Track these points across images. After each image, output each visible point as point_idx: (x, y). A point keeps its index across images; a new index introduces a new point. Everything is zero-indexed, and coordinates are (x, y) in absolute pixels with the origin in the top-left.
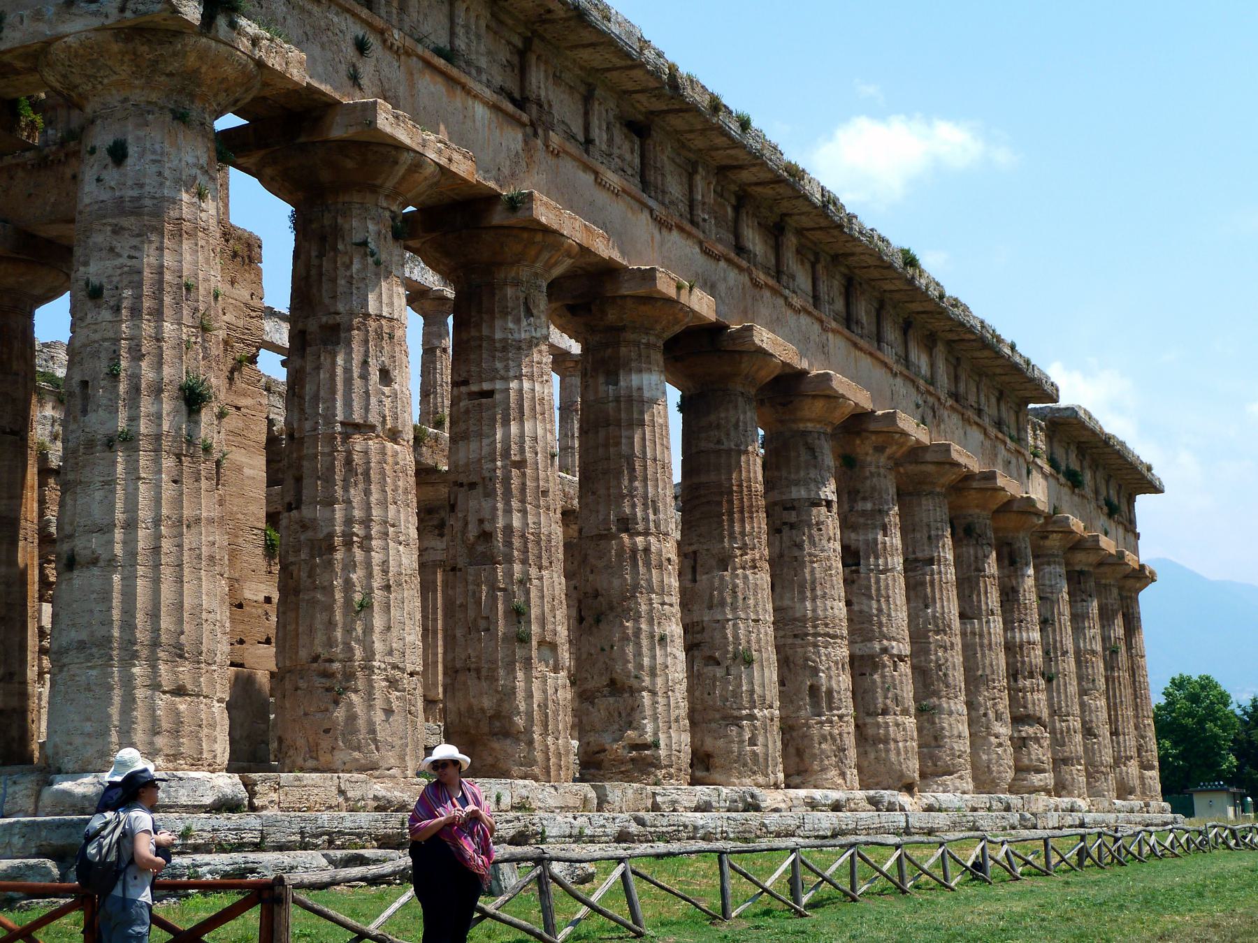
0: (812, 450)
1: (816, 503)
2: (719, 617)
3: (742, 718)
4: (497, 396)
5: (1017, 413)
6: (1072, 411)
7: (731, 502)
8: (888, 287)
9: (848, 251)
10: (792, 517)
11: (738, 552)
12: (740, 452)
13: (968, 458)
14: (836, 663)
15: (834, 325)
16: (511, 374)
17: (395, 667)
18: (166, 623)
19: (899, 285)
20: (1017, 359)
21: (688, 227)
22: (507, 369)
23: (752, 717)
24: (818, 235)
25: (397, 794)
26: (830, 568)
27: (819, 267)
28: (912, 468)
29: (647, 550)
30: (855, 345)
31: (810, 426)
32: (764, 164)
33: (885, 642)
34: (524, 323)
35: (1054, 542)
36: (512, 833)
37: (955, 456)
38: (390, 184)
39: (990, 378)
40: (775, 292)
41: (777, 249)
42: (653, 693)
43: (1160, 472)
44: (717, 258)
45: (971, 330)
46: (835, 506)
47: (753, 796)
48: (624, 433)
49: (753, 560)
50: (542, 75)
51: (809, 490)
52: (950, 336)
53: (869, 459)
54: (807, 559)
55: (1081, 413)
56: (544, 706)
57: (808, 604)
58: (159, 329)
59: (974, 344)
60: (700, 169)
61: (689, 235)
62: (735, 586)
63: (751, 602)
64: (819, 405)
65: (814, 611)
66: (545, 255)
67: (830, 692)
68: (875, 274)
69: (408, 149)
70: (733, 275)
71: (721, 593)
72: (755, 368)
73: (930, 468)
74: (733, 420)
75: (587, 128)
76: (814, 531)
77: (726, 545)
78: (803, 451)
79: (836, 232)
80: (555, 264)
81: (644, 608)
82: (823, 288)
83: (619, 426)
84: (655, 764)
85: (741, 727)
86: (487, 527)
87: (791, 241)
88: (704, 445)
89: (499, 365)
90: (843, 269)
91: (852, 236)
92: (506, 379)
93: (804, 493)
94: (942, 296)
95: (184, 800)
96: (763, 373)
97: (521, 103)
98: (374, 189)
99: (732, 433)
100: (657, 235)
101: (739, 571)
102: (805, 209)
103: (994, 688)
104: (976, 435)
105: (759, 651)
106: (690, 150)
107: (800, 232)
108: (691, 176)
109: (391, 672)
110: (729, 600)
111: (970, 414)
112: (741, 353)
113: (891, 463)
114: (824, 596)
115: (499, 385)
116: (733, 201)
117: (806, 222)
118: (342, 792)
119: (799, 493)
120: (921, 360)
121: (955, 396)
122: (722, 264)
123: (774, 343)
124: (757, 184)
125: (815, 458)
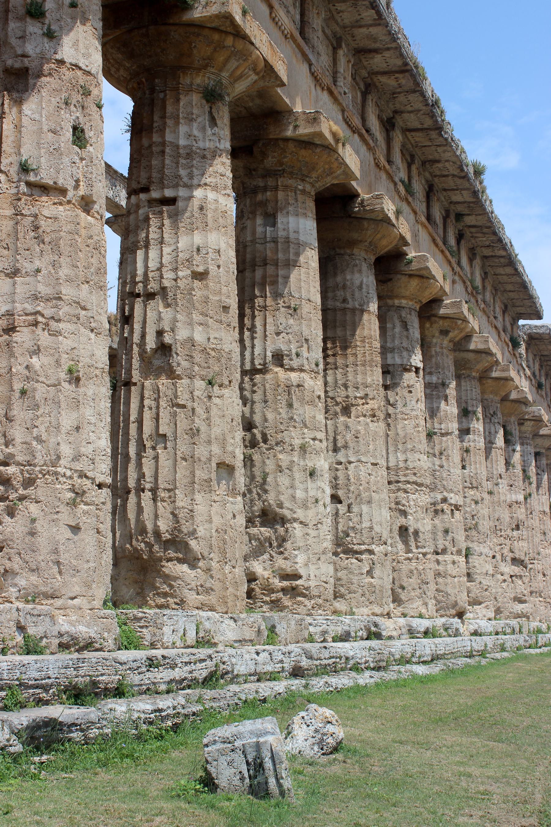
3: (361, 553)
4: (180, 204)
8: (457, 197)
9: (437, 158)
12: (362, 311)
16: (195, 182)
17: (83, 475)
22: (191, 176)
24: (419, 137)
25: (82, 629)
27: (414, 168)
31: (404, 302)
33: (445, 494)
34: (209, 132)
36: (205, 673)
46: (421, 372)
47: (376, 625)
48: (281, 272)
51: (402, 357)
52: (487, 252)
53: (434, 340)
59: (502, 260)
64: (414, 283)
66: (233, 64)
67: (416, 533)
68: (450, 183)
72: (379, 236)
73: (471, 356)
74: (357, 283)
78: (398, 324)
79: (434, 134)
80: (241, 77)
83: (276, 265)
86: (167, 339)
89: (183, 172)
90: (427, 174)
92: (190, 187)
93: (398, 361)
94: (492, 213)
96: (384, 242)
99: (357, 294)
102: (418, 105)
103: (501, 536)
107: (406, 130)
109: (78, 481)
113: (451, 345)
115: (182, 192)
116: (362, 86)
117: (413, 121)
118: (21, 628)
124: (384, 73)
125: (407, 330)
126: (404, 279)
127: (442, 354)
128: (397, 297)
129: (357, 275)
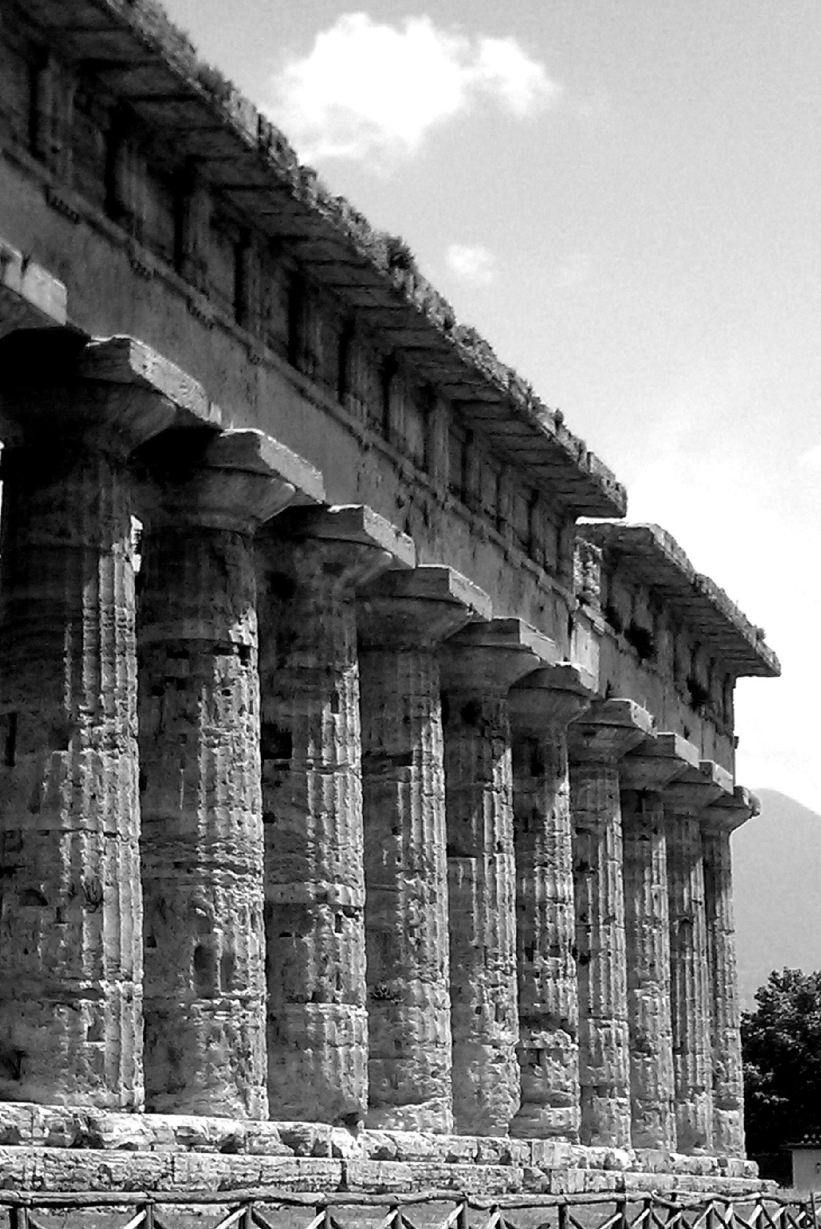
0: (220, 561)
1: (224, 649)
2: (48, 825)
5: (559, 530)
6: (645, 534)
7: (78, 634)
8: (363, 300)
10: (183, 670)
11: (86, 720)
12: (97, 553)
13: (474, 594)
14: (242, 912)
15: (268, 354)
19: (379, 298)
20: (564, 440)
21: (26, 159)
23: (96, 994)
24: (247, 200)
26: (240, 757)
27: (250, 255)
28: (385, 606)
30: (302, 392)
31: (219, 520)
32: (162, 65)
33: (324, 884)
37: (454, 589)
39: (518, 468)
40: (171, 288)
41: (180, 215)
43: (775, 643)
44: (74, 218)
45: (493, 385)
46: (254, 656)
49: (112, 734)
51: (212, 626)
52: (461, 394)
53: (315, 583)
54: (204, 739)
55: (660, 538)
57: (201, 814)
59: (496, 409)
60: (52, 62)
61: (27, 173)
62: (79, 775)
63: (105, 803)
64: (238, 483)
65: (210, 825)
67: (229, 960)
68: (340, 275)
70: (100, 249)
71: (54, 786)
72: (129, 412)
73: (414, 607)
74: (89, 497)
76: (218, 696)
77: (67, 706)
78: (206, 563)
79: (278, 197)
82: (253, 292)
85: (77, 1010)
87: (203, 206)
88: (36, 536)
90: (288, 263)
91: (306, 206)
94: (448, 324)
99: (86, 521)
101: (87, 751)
102: (228, 150)
104: (490, 557)
105: (115, 885)
106: (35, 24)
107: (218, 191)
110: (67, 798)
111: (485, 526)
112: (109, 385)
113: (351, 593)
114: (228, 803)
117: (230, 174)
119: (195, 630)
120: (408, 426)
121: (461, 493)
123: (165, 374)
125: (226, 574)
126: (220, 478)
127: (330, 611)
128: (205, 509)
129: (87, 485)
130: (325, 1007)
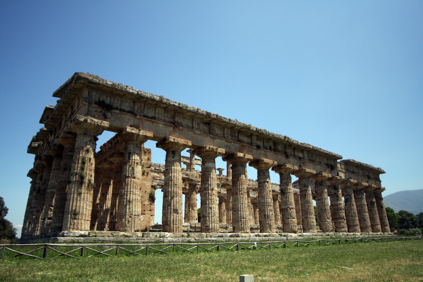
5: (334, 162)
18: (74, 208)
20: (326, 152)
23: (241, 221)
27: (264, 141)
29: (209, 193)
31: (263, 169)
35: (348, 184)
38: (135, 139)
42: (209, 217)
50: (179, 118)
56: (173, 220)
58: (78, 165)
67: (268, 215)
69: (135, 133)
73: (303, 174)
75: (193, 125)
81: (208, 202)
84: (209, 229)
95: (71, 235)
97: (174, 123)
98: (133, 140)
100: (212, 140)
108: (224, 130)
122: (232, 143)
130: (290, 220)
